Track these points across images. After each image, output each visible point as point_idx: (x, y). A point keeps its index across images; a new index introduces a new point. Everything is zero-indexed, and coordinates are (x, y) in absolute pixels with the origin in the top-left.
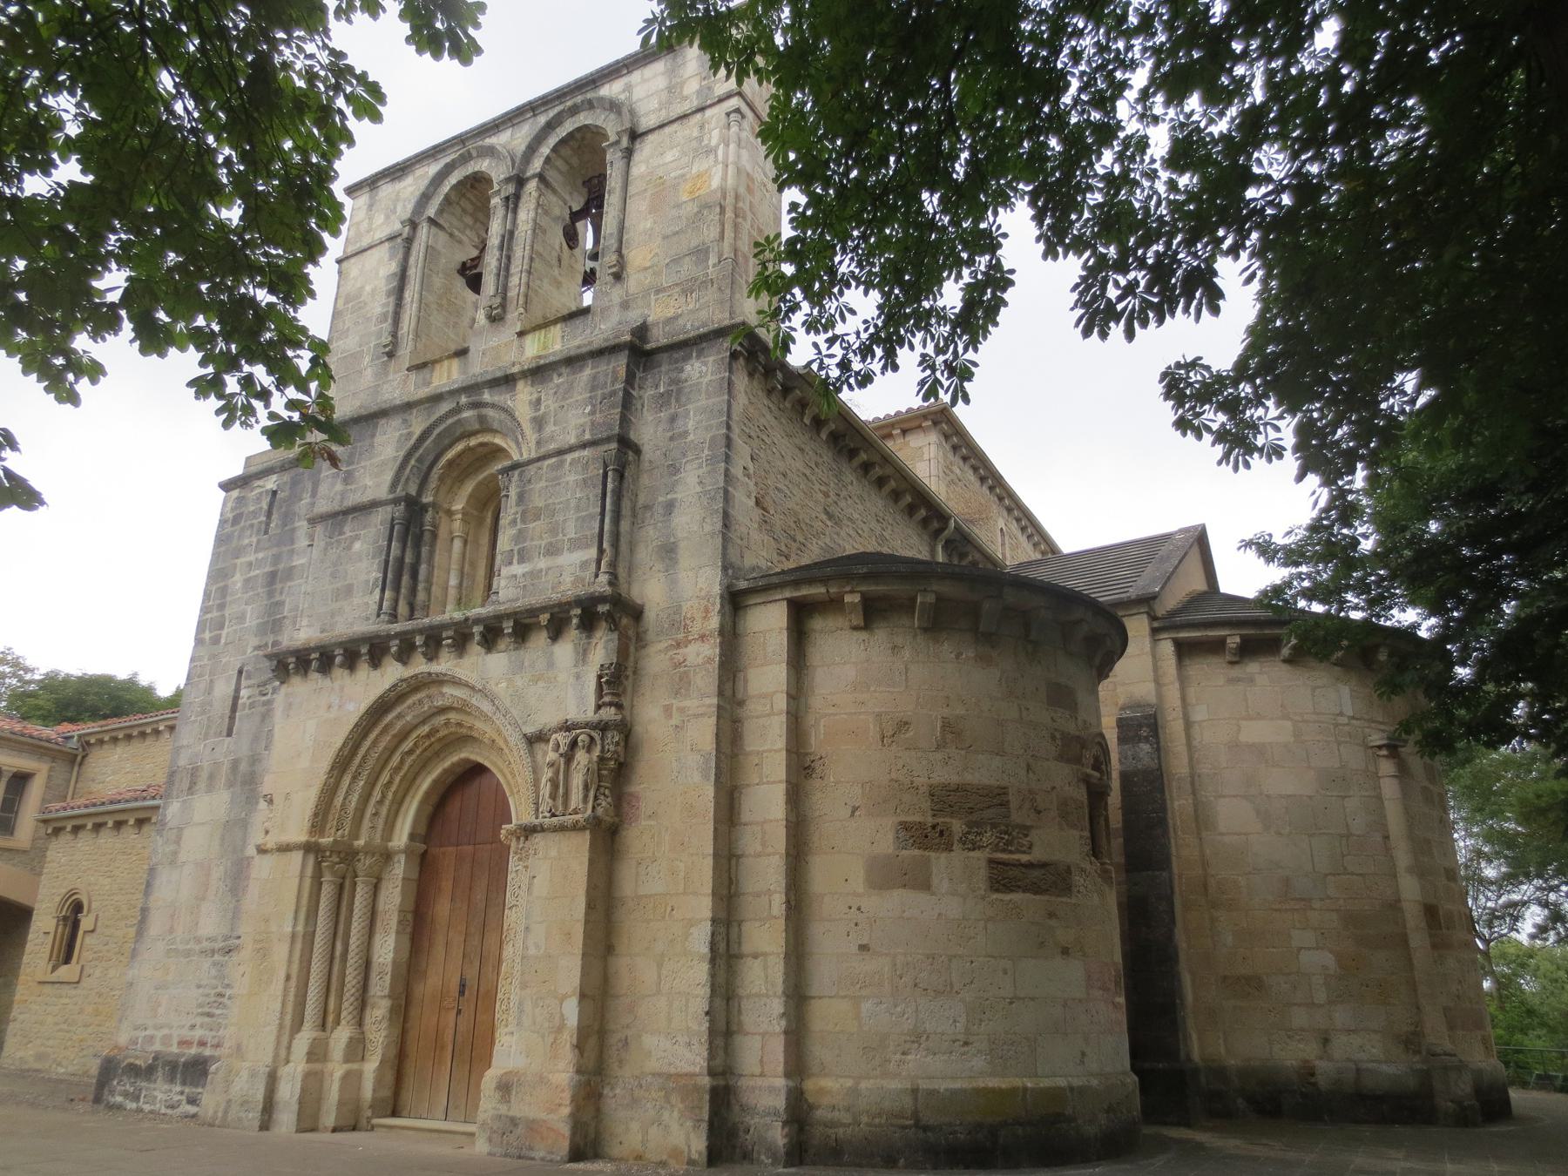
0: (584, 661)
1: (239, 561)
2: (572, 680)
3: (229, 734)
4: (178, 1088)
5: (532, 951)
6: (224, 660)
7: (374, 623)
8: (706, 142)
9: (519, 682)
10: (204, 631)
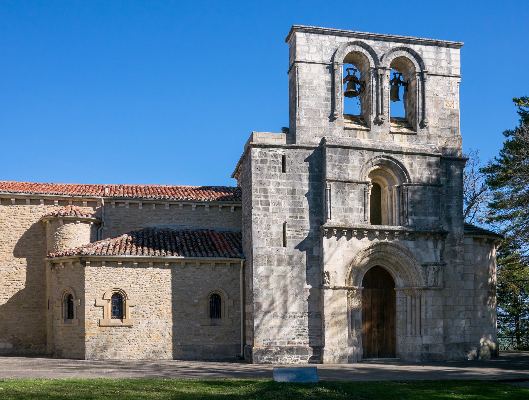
0: (436, 248)
1: (271, 180)
2: (433, 252)
3: (285, 245)
4: (296, 356)
5: (429, 317)
6: (274, 219)
7: (363, 223)
8: (451, 90)
9: (418, 250)
10: (258, 204)
